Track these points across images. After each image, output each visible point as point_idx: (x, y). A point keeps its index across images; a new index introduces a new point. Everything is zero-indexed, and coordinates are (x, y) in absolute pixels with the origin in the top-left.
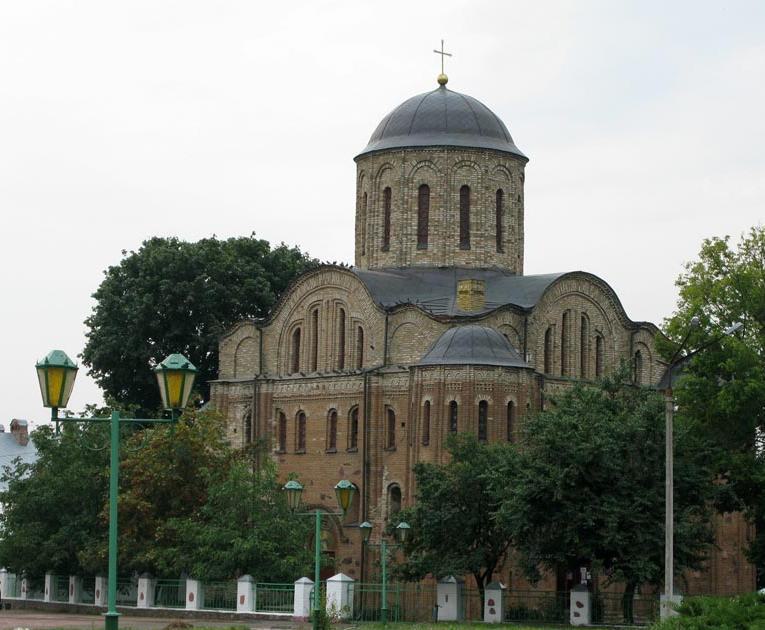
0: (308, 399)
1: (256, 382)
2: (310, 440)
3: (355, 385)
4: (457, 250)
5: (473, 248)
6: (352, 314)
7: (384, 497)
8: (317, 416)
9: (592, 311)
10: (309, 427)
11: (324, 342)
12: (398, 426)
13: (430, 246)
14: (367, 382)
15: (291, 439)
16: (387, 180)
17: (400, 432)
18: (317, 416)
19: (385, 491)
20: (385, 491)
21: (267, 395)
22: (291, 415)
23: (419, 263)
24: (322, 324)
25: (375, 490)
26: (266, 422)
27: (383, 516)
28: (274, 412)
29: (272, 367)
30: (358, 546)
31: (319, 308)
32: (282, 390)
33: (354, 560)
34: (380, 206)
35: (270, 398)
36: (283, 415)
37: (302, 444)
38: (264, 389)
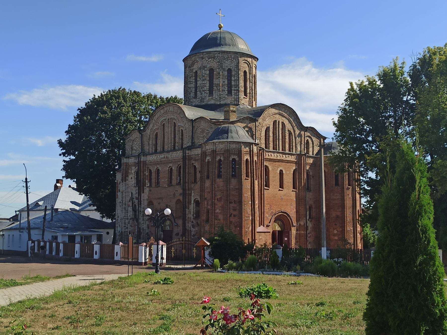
0: (161, 163)
1: (139, 156)
2: (162, 181)
3: (179, 154)
4: (226, 96)
5: (233, 96)
6: (178, 124)
7: (192, 205)
8: (164, 169)
9: (286, 122)
10: (161, 175)
11: (167, 137)
12: (198, 172)
13: (214, 96)
14: (184, 153)
15: (153, 181)
16: (195, 67)
17: (198, 175)
18: (164, 169)
19: (192, 202)
20: (192, 202)
21: (143, 161)
22: (153, 169)
23: (210, 103)
24: (166, 129)
25: (188, 202)
26: (143, 173)
27: (192, 213)
28: (147, 169)
29: (146, 148)
30: (181, 228)
31: (165, 122)
32: (150, 158)
33: (180, 234)
34: (193, 80)
35: (144, 162)
36: (150, 170)
37: (158, 183)
38: (143, 159)
